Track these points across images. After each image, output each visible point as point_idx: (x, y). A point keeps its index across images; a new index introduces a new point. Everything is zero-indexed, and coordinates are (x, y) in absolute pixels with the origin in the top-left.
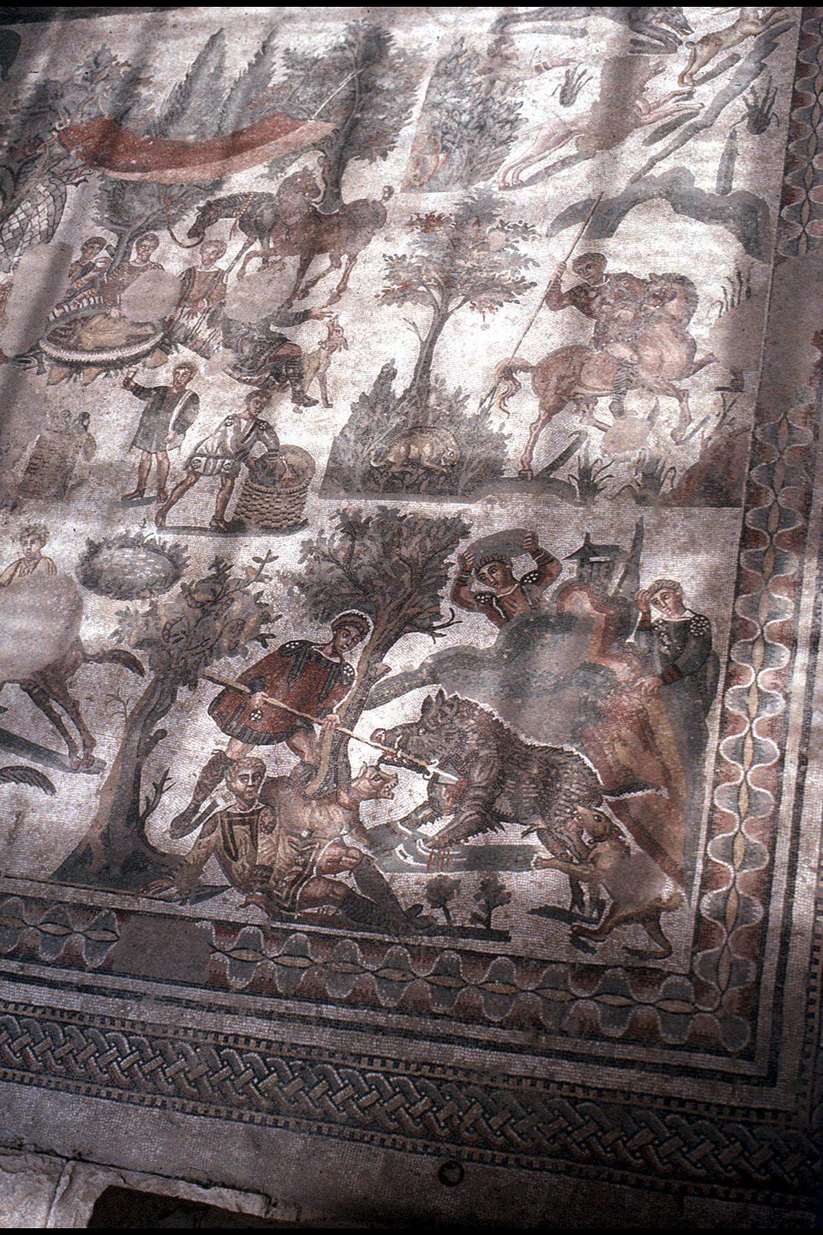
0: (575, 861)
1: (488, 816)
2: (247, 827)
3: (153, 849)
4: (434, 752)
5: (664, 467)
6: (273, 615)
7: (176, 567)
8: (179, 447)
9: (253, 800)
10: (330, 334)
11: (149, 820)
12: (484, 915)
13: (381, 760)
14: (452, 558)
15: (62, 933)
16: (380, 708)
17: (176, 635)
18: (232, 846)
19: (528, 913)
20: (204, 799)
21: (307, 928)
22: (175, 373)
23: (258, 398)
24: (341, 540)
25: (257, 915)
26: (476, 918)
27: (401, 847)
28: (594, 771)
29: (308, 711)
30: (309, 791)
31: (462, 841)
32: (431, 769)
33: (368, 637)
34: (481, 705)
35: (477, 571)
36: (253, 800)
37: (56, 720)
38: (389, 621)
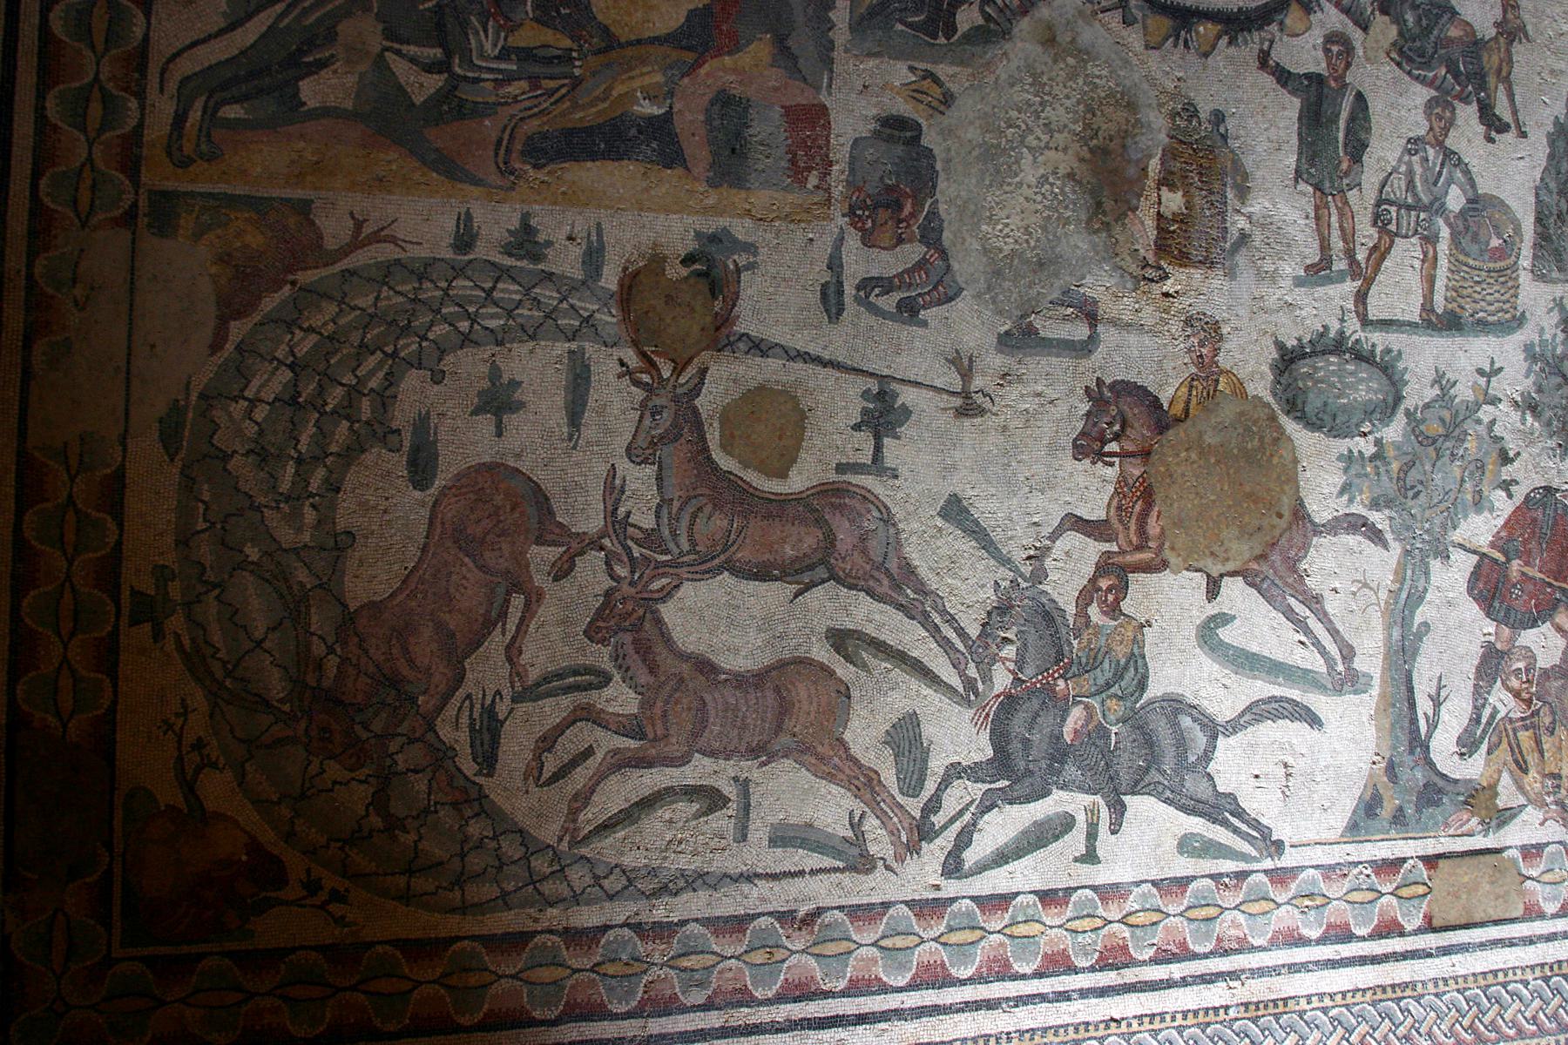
3: (1444, 776)
6: (1511, 454)
7: (1394, 384)
8: (1360, 184)
10: (1505, 12)
17: (1413, 487)
20: (1483, 706)
22: (1327, 51)
23: (1438, 110)
24: (1563, 344)
37: (1300, 625)
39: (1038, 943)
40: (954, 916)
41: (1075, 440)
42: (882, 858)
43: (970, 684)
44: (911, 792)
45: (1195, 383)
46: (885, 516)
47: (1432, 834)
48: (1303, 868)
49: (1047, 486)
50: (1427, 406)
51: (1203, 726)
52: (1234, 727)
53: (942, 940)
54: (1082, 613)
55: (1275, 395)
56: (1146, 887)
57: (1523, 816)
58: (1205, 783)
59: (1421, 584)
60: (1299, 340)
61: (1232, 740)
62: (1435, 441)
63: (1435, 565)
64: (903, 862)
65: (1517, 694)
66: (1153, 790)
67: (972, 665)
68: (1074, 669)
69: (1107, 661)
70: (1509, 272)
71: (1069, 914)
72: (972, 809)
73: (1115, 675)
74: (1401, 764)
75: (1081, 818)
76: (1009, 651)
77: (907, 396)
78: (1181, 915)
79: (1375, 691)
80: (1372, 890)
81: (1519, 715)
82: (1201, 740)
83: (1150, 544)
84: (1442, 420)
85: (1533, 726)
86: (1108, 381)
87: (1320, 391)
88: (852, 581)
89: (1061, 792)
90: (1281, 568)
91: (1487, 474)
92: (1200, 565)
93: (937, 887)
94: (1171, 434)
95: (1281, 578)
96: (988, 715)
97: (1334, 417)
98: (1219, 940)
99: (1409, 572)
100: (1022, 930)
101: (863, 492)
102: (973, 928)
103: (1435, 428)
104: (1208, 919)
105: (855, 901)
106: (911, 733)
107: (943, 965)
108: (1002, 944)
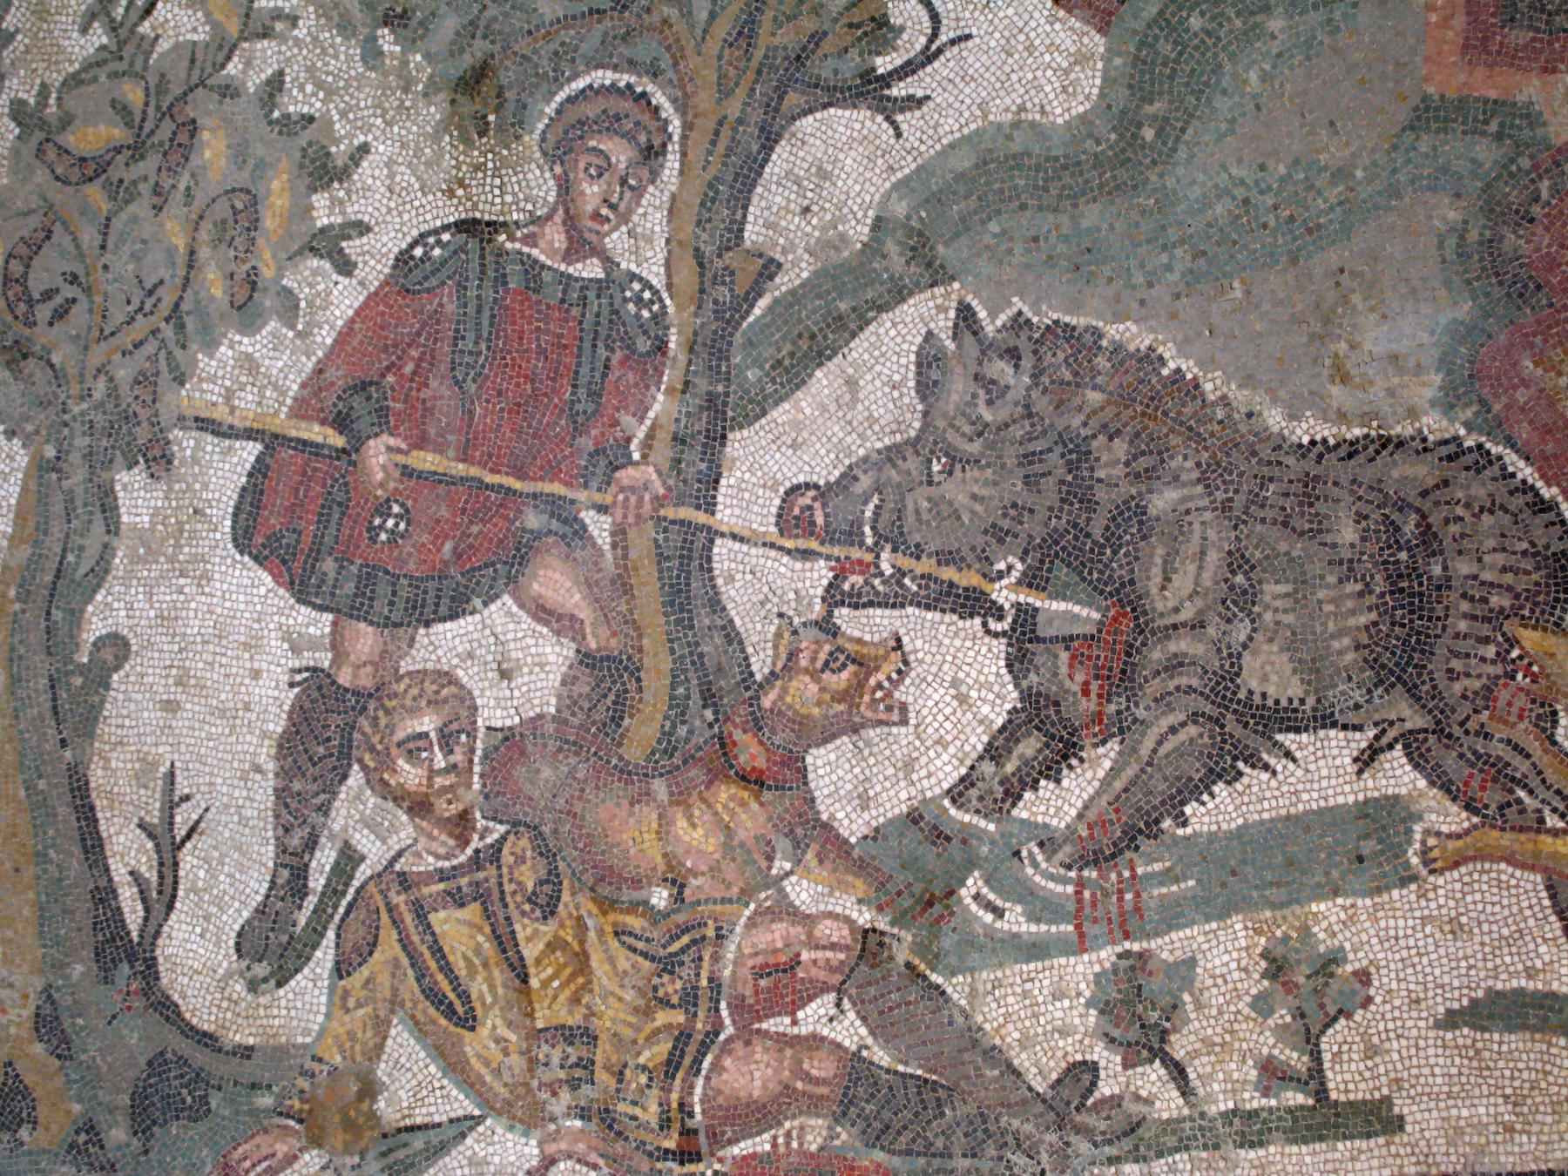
0: (1552, 821)
1: (1231, 725)
2: (472, 912)
3: (206, 1039)
4: (999, 535)
6: (340, 151)
9: (464, 817)
12: (1297, 1060)
13: (834, 596)
16: (781, 413)
17: (48, 295)
18: (445, 985)
19: (1438, 1025)
20: (311, 844)
26: (1273, 1074)
27: (973, 883)
29: (552, 472)
30: (634, 753)
31: (1167, 824)
32: (1004, 594)
33: (672, 162)
34: (1114, 331)
36: (464, 817)
38: (724, 91)
62: (102, 169)
65: (419, 806)
74: (79, 1011)
84: (121, 109)
91: (269, 223)
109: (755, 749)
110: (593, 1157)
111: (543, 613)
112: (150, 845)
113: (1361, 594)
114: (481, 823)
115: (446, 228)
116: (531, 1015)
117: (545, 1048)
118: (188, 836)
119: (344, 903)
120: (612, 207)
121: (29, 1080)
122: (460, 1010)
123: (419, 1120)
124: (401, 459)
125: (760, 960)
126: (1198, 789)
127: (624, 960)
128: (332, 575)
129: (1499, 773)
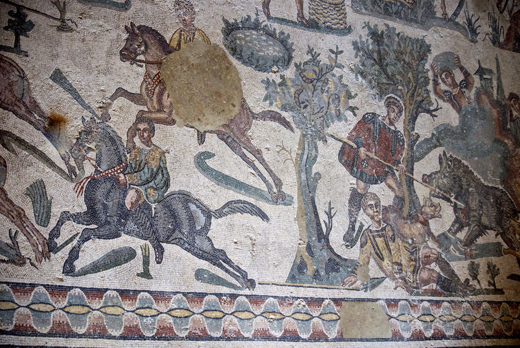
2: (382, 239)
3: (338, 256)
4: (452, 190)
5: (498, 26)
6: (353, 94)
7: (287, 50)
11: (331, 238)
14: (427, 66)
15: (307, 319)
17: (303, 103)
18: (378, 252)
20: (355, 221)
21: (427, 298)
25: (401, 294)
28: (513, 200)
29: (389, 161)
31: (475, 241)
32: (452, 199)
35: (441, 76)
37: (251, 164)
39: (121, 319)
40: (72, 297)
41: (121, 51)
42: (29, 259)
43: (72, 170)
44: (42, 224)
45: (183, 33)
46: (22, 75)
47: (336, 287)
48: (268, 297)
49: (107, 72)
50: (306, 63)
51: (203, 211)
52: (220, 213)
53: (66, 310)
54: (130, 140)
55: (225, 45)
56: (180, 296)
57: (384, 283)
58: (206, 243)
59: (314, 152)
60: (236, 20)
61: (220, 220)
62: (312, 82)
63: (320, 144)
64: (41, 262)
65: (372, 218)
66: (179, 242)
67: (72, 159)
68: (129, 169)
69: (146, 168)
70: (340, 6)
71: (137, 305)
72: (77, 238)
73: (151, 176)
74: (315, 247)
75: (139, 252)
76: (92, 155)
77: (32, 17)
78: (201, 314)
79: (296, 205)
80: (307, 314)
81: (375, 229)
82: (202, 219)
83: (165, 110)
84: (314, 71)
85: (382, 236)
86: (137, 25)
87: (249, 48)
88: (5, 105)
89: (127, 236)
90: (237, 133)
91: (341, 102)
92: (194, 124)
93: (62, 280)
94: (172, 55)
95: (238, 138)
96: (82, 187)
97: (258, 61)
98: (224, 331)
99: (306, 146)
100: (110, 310)
101: (10, 61)
102: (83, 306)
103: (311, 75)
104: (217, 318)
105: (15, 280)
106: (41, 191)
107: (67, 324)
108: (100, 317)
109: (422, 218)
110: (403, 287)
111: (390, 187)
112: (327, 216)
113: (494, 210)
114: (382, 223)
115: (371, 113)
116: (392, 259)
117: (395, 266)
118: (334, 215)
119: (361, 233)
120: (396, 118)
121: (306, 260)
122: (381, 257)
123: (376, 277)
124: (366, 153)
125: (425, 255)
126: (477, 236)
127: (406, 252)
128: (356, 171)
129: (510, 240)
